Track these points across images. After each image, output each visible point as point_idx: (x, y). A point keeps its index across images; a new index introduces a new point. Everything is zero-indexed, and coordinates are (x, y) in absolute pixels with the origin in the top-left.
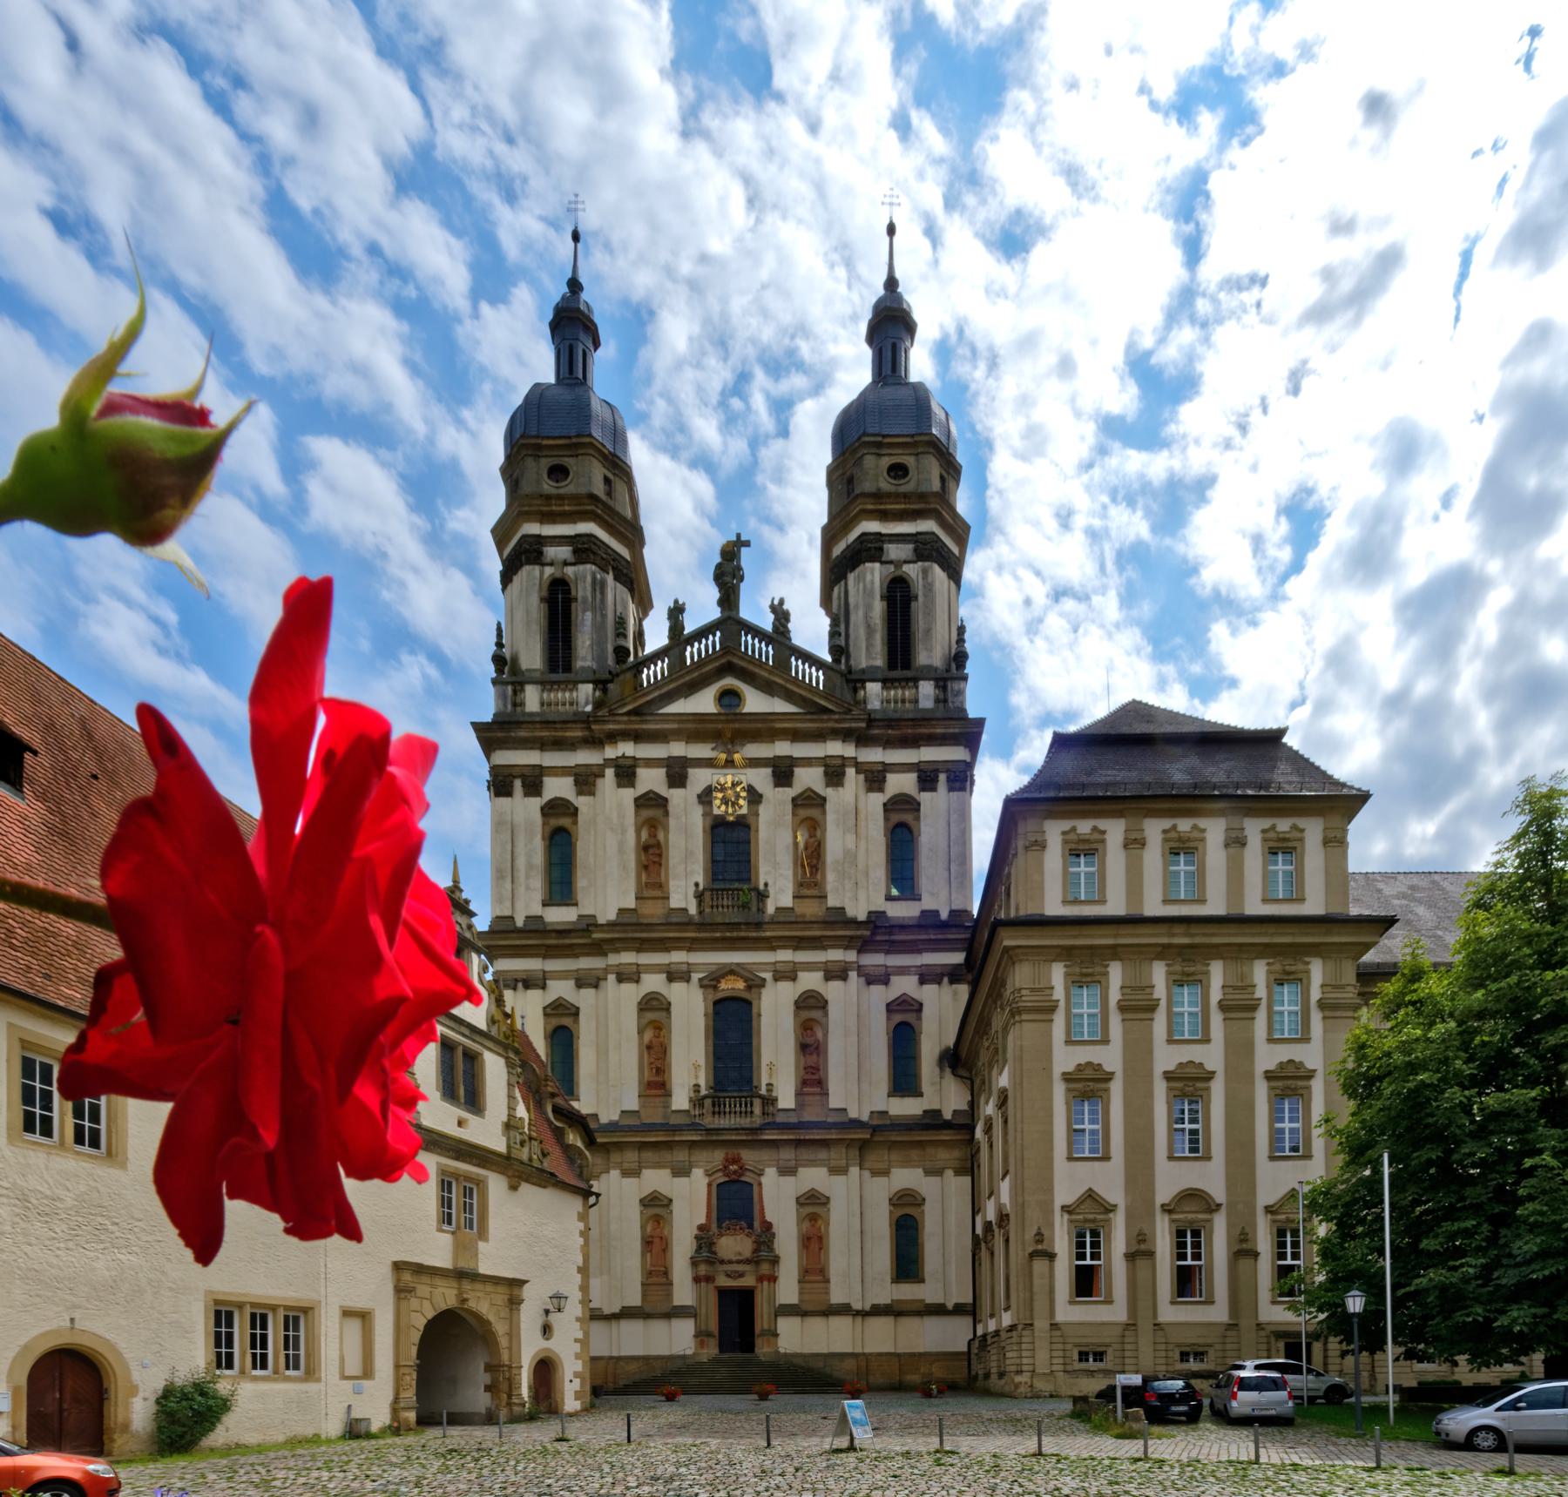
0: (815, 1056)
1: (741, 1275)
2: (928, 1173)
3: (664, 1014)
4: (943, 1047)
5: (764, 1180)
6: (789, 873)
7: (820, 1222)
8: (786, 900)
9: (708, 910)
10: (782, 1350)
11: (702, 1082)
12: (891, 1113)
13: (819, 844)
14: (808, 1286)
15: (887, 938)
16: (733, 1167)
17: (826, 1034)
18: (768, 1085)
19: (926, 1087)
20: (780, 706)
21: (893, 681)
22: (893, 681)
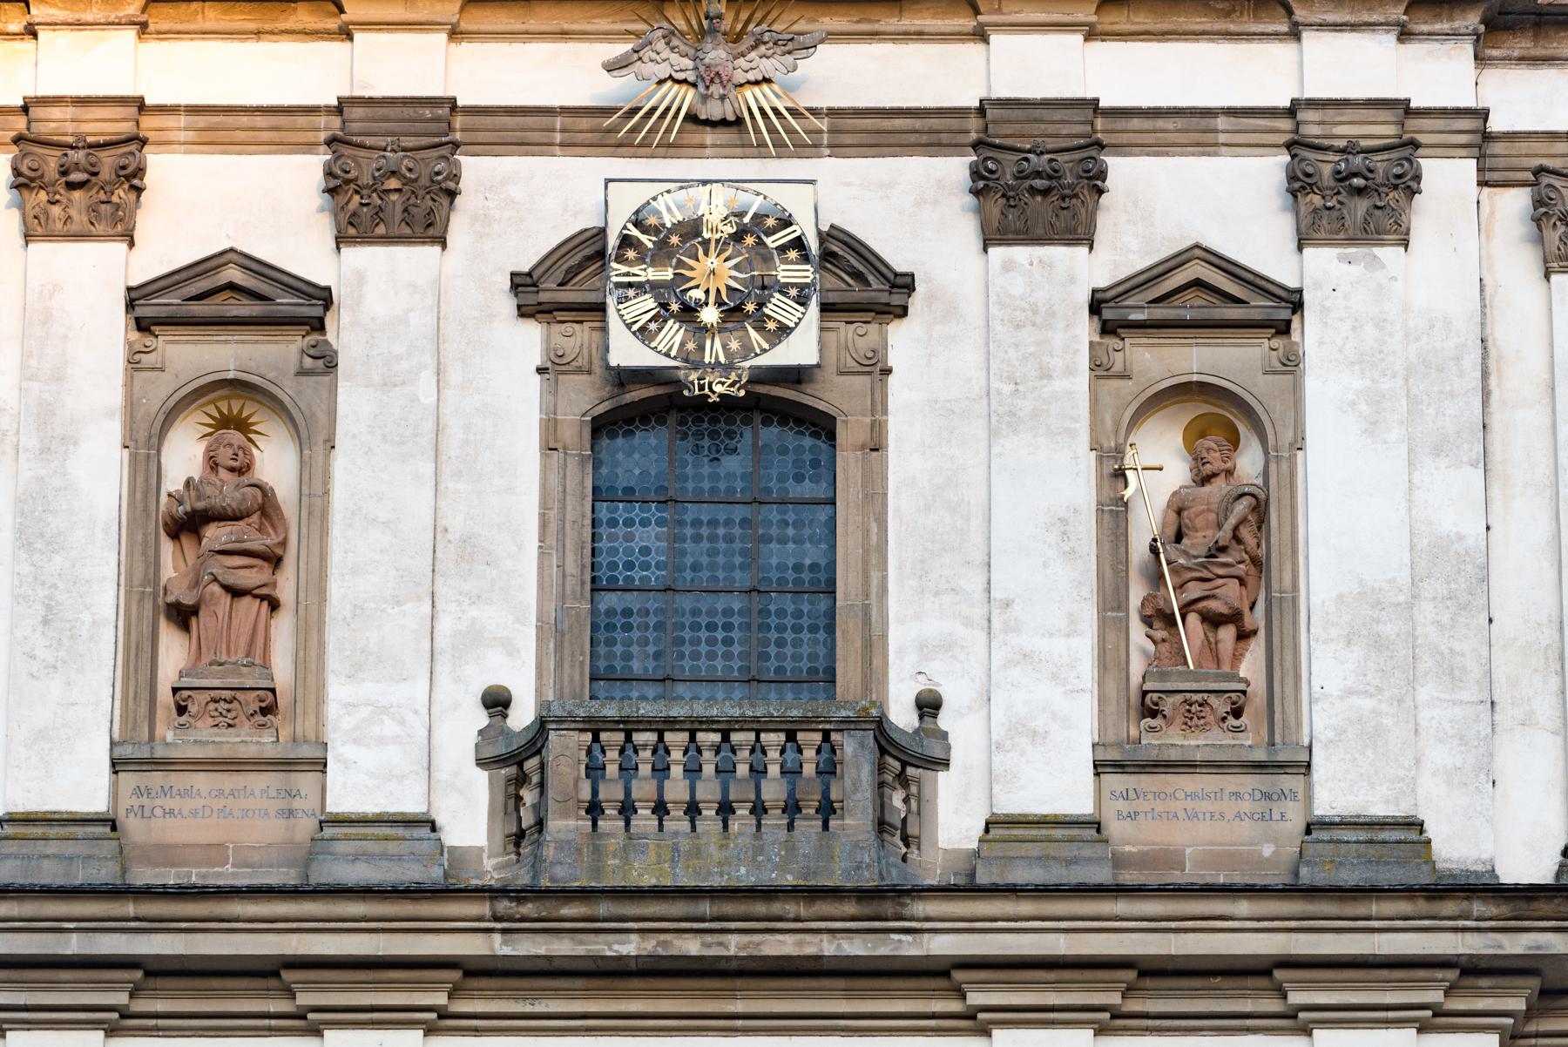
6: (1083, 648)
9: (565, 825)
13: (1260, 510)
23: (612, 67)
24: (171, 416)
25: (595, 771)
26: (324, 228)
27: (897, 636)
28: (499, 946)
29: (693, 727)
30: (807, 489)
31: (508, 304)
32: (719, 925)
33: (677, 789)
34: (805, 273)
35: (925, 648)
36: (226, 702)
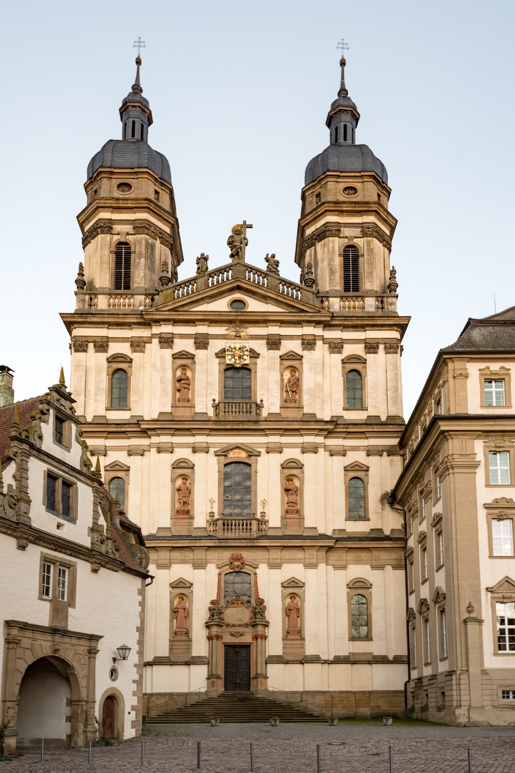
0: (294, 496)
1: (241, 635)
2: (373, 568)
3: (190, 470)
4: (383, 492)
5: (257, 571)
6: (279, 395)
7: (297, 599)
8: (276, 409)
9: (222, 414)
10: (270, 689)
11: (216, 510)
12: (347, 531)
13: (298, 380)
14: (288, 642)
15: (345, 430)
16: (237, 563)
17: (302, 484)
18: (261, 513)
19: (371, 515)
20: (271, 308)
21: (347, 297)
22: (347, 297)
23: (226, 330)
24: (177, 369)
25: (225, 408)
26: (194, 348)
27: (258, 393)
28: (214, 427)
29: (236, 403)
30: (248, 377)
31: (215, 356)
32: (239, 425)
33: (234, 410)
34: (248, 353)
35: (261, 395)
36: (184, 400)
